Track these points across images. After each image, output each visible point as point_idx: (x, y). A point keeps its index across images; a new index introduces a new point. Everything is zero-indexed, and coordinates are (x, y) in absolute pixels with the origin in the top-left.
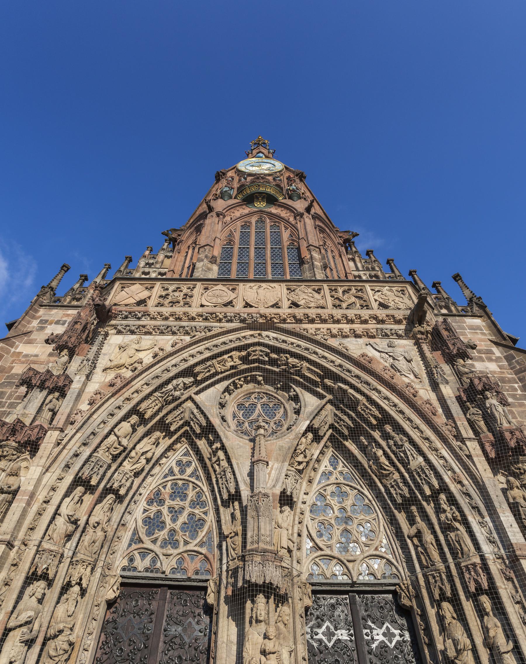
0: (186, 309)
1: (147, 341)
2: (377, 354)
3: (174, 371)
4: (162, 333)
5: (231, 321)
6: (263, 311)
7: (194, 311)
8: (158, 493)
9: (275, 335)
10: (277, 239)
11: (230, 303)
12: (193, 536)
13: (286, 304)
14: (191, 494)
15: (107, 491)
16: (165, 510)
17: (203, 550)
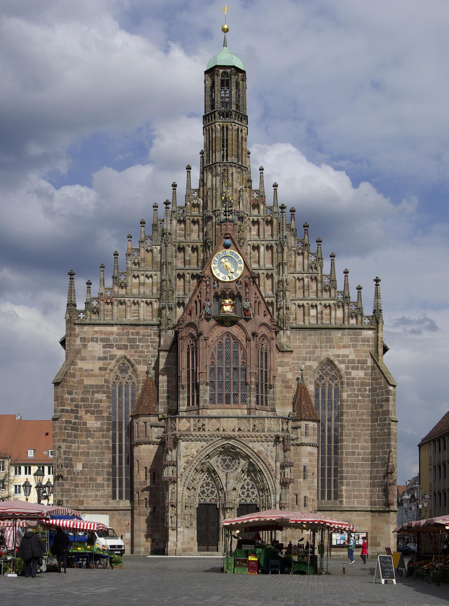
0: (204, 433)
1: (193, 444)
2: (263, 449)
3: (204, 456)
4: (197, 441)
5: (219, 437)
6: (229, 433)
7: (206, 433)
8: (202, 485)
10: (236, 353)
11: (218, 430)
12: (213, 495)
13: (237, 429)
14: (211, 485)
15: (193, 488)
16: (205, 490)
17: (215, 498)
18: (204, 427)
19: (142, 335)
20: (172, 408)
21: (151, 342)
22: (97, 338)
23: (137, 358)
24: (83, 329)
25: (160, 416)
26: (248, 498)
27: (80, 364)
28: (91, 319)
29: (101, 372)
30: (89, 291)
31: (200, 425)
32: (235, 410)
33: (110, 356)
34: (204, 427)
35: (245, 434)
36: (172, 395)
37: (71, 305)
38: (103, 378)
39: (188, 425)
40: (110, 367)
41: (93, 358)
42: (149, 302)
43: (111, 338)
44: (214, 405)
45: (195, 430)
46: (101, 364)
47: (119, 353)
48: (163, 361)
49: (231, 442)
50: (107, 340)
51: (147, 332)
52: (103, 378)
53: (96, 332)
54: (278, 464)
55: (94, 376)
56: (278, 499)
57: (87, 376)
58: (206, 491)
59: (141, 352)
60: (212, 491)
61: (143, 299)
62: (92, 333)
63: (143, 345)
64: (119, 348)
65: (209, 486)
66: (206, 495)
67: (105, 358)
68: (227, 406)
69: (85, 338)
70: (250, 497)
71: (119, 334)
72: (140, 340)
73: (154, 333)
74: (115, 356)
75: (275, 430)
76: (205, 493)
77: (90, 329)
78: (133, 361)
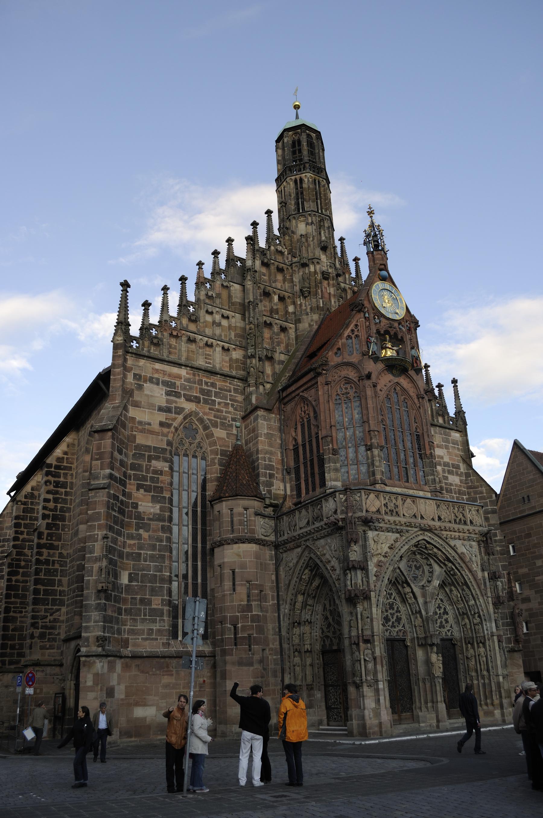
4: (388, 532)
7: (403, 520)
9: (429, 535)
11: (415, 516)
13: (437, 518)
18: (397, 510)
19: (219, 389)
20: (278, 492)
21: (230, 400)
22: (158, 379)
23: (213, 418)
24: (139, 362)
25: (268, 501)
26: (442, 630)
27: (132, 412)
28: (149, 351)
29: (163, 429)
30: (146, 315)
31: (391, 506)
32: (418, 492)
33: (176, 407)
34: (397, 510)
35: (448, 525)
36: (277, 473)
37: (123, 324)
38: (165, 439)
39: (377, 504)
40: (175, 424)
41: (151, 406)
42: (226, 348)
43: (178, 383)
44: (391, 481)
45: (386, 513)
46: (162, 417)
47: (189, 407)
48: (262, 423)
49: (428, 536)
50: (173, 385)
51: (226, 386)
52: (165, 439)
53: (157, 371)
54: (486, 574)
55: (151, 432)
56: (494, 630)
57: (143, 431)
58: (390, 617)
59: (218, 410)
60: (397, 616)
61: (219, 342)
62: (151, 370)
63: (221, 402)
64: (189, 399)
65: (393, 609)
66: (390, 623)
67: (168, 410)
68: (407, 484)
69: (140, 376)
70: (444, 628)
71: (188, 380)
72: (217, 395)
73: (234, 389)
74: (183, 409)
75: (478, 524)
76: (389, 620)
77: (148, 365)
78: (208, 421)
